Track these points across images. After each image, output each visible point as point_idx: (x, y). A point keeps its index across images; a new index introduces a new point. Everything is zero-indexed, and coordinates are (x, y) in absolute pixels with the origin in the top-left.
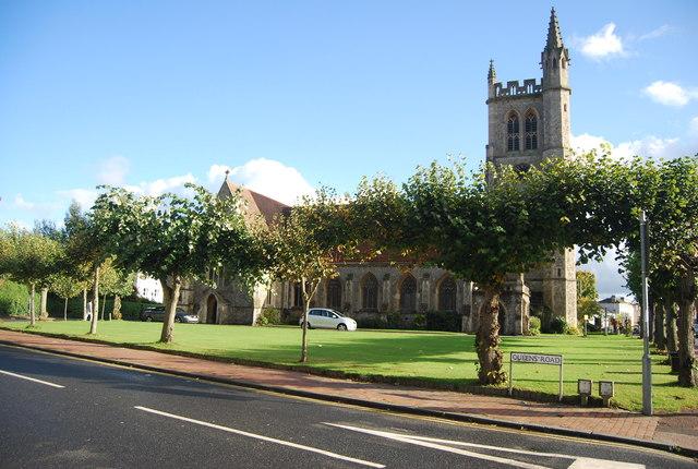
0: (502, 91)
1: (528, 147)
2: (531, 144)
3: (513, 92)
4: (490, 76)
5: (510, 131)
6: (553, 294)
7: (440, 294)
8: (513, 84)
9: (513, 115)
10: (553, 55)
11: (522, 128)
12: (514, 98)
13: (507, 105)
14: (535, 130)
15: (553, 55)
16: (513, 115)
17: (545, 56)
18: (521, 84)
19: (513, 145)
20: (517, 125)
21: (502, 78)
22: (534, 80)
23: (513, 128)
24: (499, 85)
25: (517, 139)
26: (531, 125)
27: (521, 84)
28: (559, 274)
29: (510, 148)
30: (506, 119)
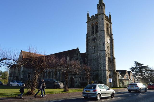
0: (90, 18)
2: (97, 32)
3: (93, 18)
4: (88, 15)
6: (99, 75)
7: (62, 76)
8: (93, 15)
9: (93, 25)
10: (101, 6)
12: (92, 20)
15: (101, 6)
16: (93, 25)
17: (99, 5)
18: (94, 16)
19: (93, 33)
21: (90, 16)
23: (93, 28)
25: (94, 31)
26: (97, 27)
27: (94, 16)
28: (101, 68)
29: (92, 34)
30: (91, 26)
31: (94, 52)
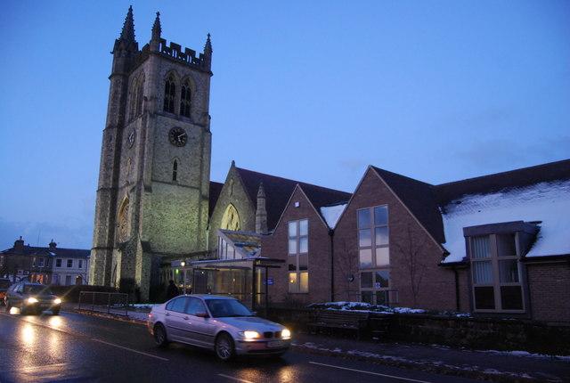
1: (182, 113)
2: (186, 112)
3: (174, 54)
5: (167, 92)
8: (176, 47)
11: (179, 94)
13: (168, 66)
14: (189, 98)
19: (169, 107)
20: (174, 86)
22: (190, 52)
23: (170, 89)
24: (164, 42)
25: (172, 103)
26: (187, 94)
29: (165, 109)
31: (175, 178)
